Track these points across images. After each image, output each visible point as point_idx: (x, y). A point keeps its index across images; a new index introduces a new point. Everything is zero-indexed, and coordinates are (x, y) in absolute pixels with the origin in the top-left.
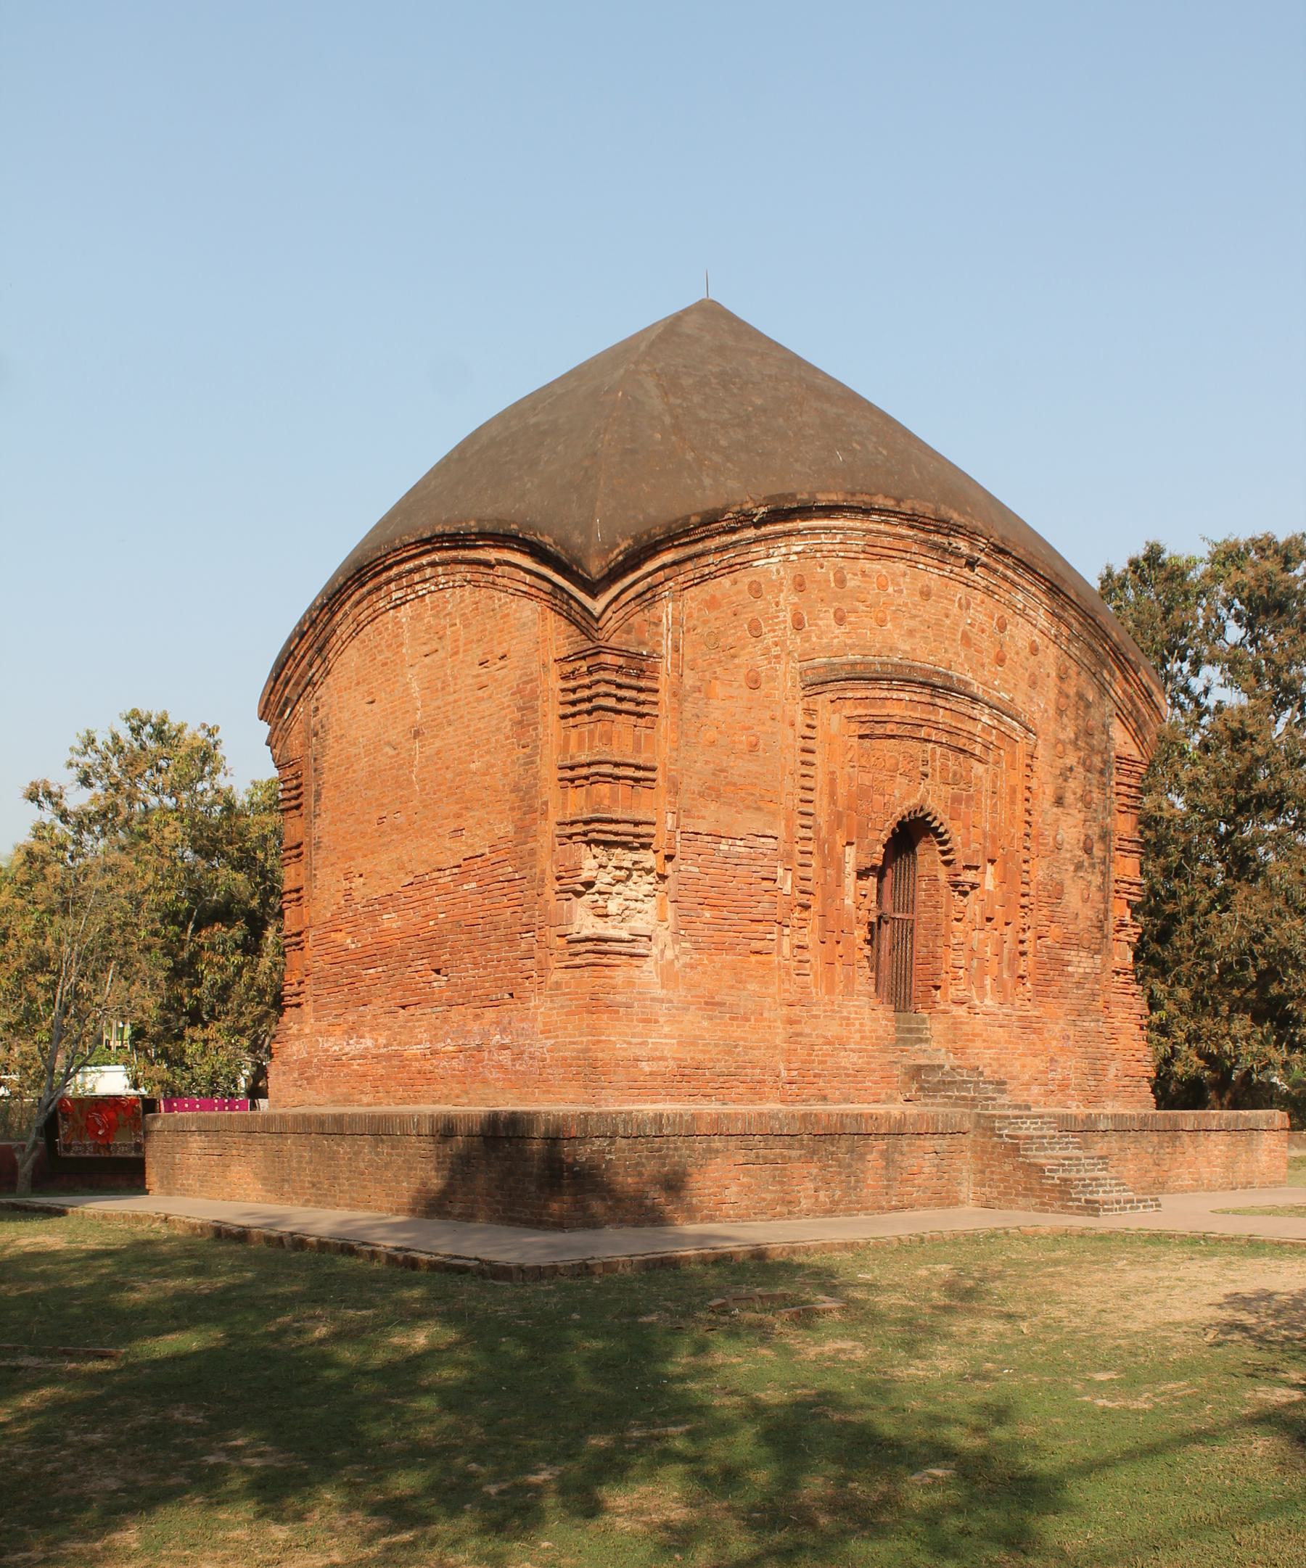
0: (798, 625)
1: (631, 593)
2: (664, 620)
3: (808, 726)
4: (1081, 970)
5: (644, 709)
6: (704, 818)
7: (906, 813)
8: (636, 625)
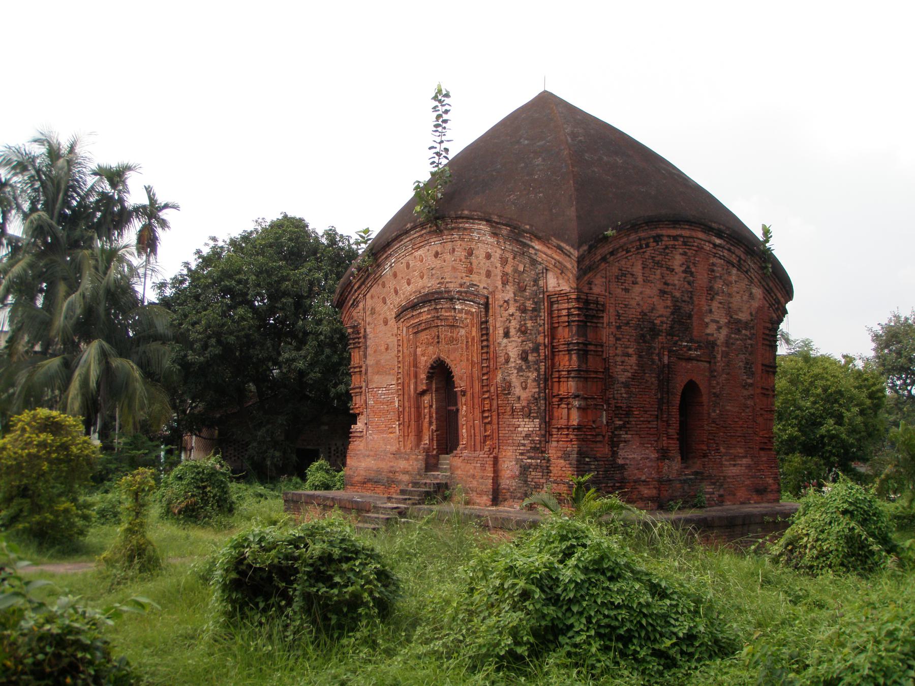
0: (396, 292)
4: (526, 429)
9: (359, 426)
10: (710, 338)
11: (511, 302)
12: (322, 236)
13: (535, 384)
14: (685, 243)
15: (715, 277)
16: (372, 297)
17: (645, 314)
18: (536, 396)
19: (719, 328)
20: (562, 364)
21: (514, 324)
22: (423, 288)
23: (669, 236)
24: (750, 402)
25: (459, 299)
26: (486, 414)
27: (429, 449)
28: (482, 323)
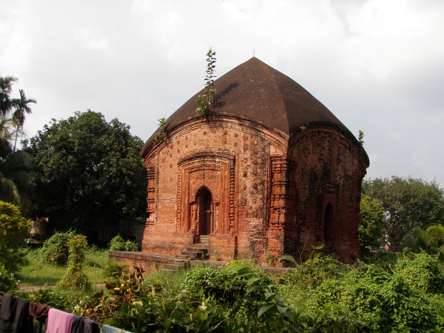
0: (179, 151)
9: (152, 218)
10: (337, 183)
11: (249, 159)
12: (110, 123)
13: (261, 200)
14: (329, 136)
15: (340, 153)
16: (163, 153)
17: (313, 169)
18: (261, 207)
19: (341, 178)
20: (276, 191)
21: (250, 170)
22: (196, 150)
23: (324, 132)
24: (350, 215)
25: (218, 157)
26: (231, 215)
27: (195, 232)
28: (231, 169)
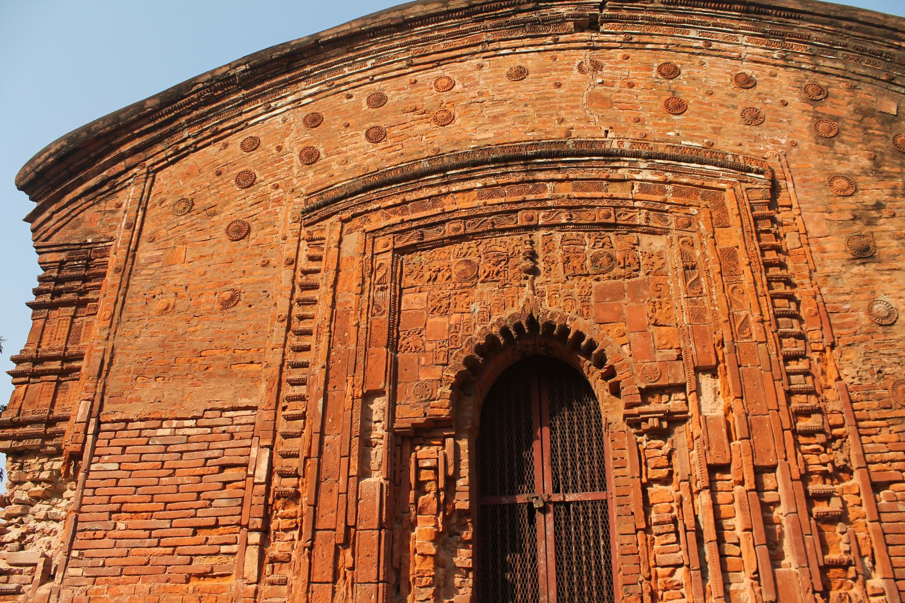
0: (310, 157)
1: (80, 190)
2: (124, 205)
3: (311, 258)
5: (90, 296)
6: (138, 399)
7: (495, 330)
8: (87, 218)
25: (648, 157)
